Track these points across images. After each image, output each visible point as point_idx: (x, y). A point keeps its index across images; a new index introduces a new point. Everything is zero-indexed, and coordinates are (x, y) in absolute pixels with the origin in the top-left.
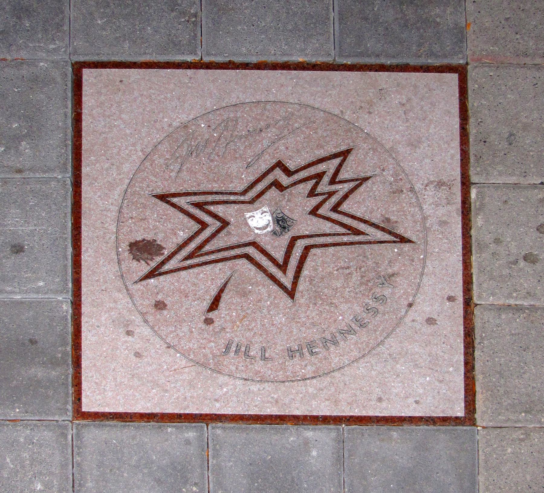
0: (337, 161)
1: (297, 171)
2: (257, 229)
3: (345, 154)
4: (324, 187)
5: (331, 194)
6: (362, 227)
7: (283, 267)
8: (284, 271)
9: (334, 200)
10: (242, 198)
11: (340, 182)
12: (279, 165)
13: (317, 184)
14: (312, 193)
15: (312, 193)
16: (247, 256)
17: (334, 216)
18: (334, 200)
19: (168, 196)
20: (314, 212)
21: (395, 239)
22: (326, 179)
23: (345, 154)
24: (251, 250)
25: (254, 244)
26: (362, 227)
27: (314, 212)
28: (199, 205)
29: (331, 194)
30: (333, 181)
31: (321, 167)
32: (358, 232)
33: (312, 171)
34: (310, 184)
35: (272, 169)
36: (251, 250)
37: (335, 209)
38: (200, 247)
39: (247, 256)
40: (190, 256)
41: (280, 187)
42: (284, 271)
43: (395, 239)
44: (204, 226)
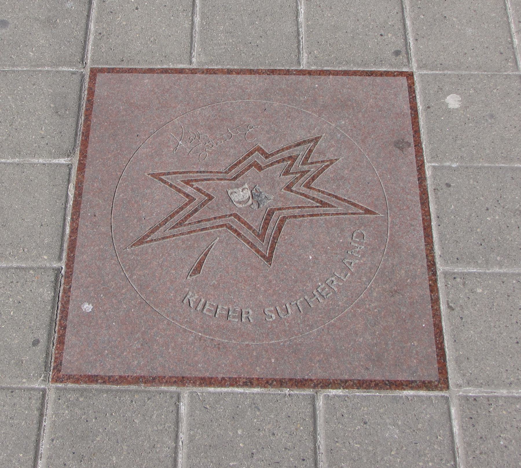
0: (306, 147)
1: (272, 155)
2: (240, 202)
3: (317, 139)
4: (298, 165)
5: (303, 173)
6: (332, 201)
7: (261, 236)
9: (306, 178)
12: (259, 149)
13: (291, 165)
15: (287, 172)
20: (288, 188)
23: (317, 139)
25: (236, 216)
26: (332, 201)
27: (288, 188)
29: (303, 173)
31: (294, 152)
32: (330, 206)
33: (286, 154)
38: (186, 218)
41: (260, 168)
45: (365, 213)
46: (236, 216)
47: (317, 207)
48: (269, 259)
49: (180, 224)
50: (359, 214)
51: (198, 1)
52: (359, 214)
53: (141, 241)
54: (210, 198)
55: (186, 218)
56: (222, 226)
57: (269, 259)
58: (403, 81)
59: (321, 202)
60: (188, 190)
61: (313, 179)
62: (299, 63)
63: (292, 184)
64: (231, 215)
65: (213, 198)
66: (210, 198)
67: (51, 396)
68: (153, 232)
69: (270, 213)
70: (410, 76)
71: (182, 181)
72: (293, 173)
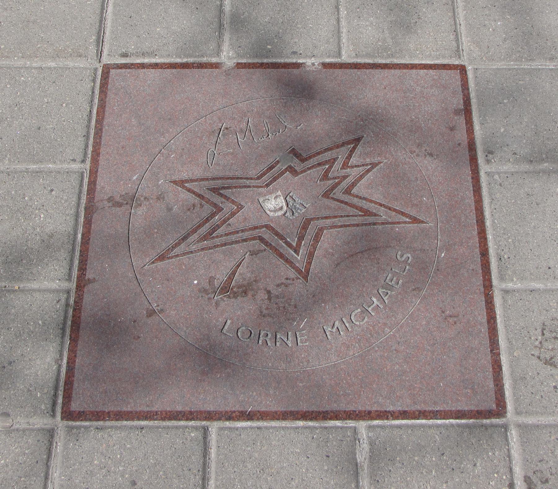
8: (297, 251)
11: (352, 167)
14: (325, 177)
16: (261, 239)
17: (346, 198)
18: (345, 184)
19: (219, 189)
20: (326, 195)
21: (360, 213)
22: (338, 165)
27: (326, 195)
28: (215, 190)
30: (345, 165)
37: (348, 191)
39: (261, 239)
40: (205, 238)
42: (297, 251)
43: (360, 213)
45: (412, 223)
48: (306, 278)
49: (208, 236)
50: (405, 222)
52: (405, 222)
53: (162, 258)
55: (214, 230)
58: (456, 75)
62: (339, 55)
65: (242, 207)
68: (174, 248)
70: (462, 69)
72: (331, 179)
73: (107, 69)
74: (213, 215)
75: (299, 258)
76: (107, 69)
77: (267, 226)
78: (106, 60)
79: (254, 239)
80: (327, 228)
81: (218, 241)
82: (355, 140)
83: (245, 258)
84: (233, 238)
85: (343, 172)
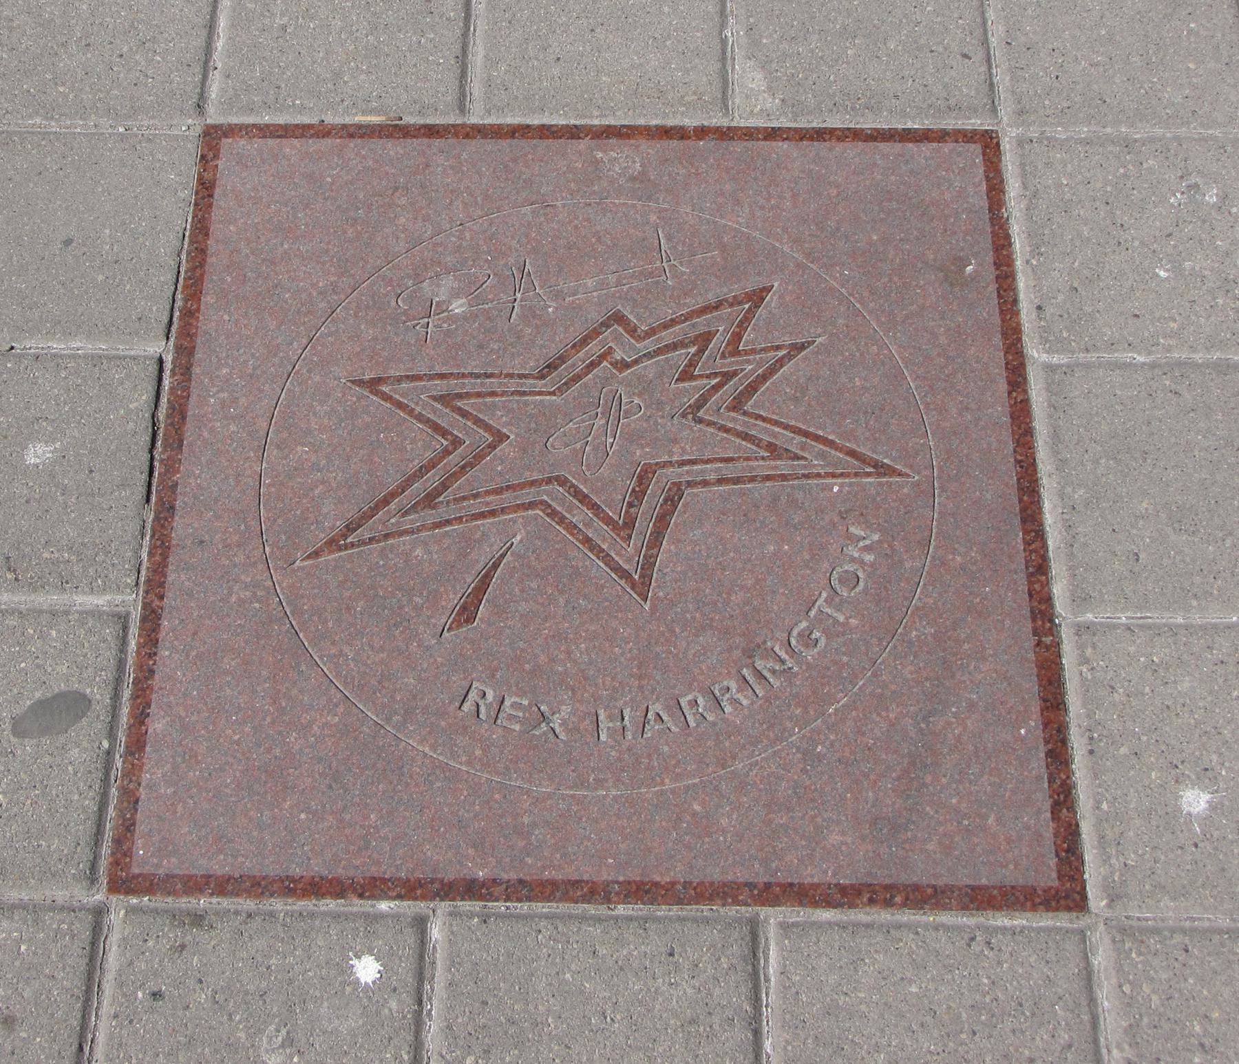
1: (652, 332)
4: (714, 360)
5: (727, 376)
10: (540, 385)
12: (619, 318)
14: (686, 375)
15: (686, 375)
17: (736, 421)
24: (553, 494)
25: (562, 481)
29: (727, 376)
30: (733, 348)
34: (681, 357)
35: (605, 324)
36: (553, 494)
37: (737, 405)
38: (444, 486)
44: (457, 442)
46: (562, 481)
47: (763, 458)
49: (429, 500)
51: (480, 5)
54: (501, 437)
55: (444, 486)
56: (531, 505)
57: (642, 587)
59: (771, 447)
60: (445, 417)
61: (752, 389)
63: (703, 400)
64: (549, 481)
66: (501, 437)
67: (116, 917)
69: (644, 476)
70: (989, 143)
71: (434, 398)
73: (213, 137)
74: (447, 452)
75: (628, 553)
76: (213, 137)
77: (557, 479)
78: (214, 116)
79: (531, 505)
80: (690, 484)
81: (443, 513)
82: (748, 297)
83: (512, 544)
84: (508, 498)
85: (723, 365)
